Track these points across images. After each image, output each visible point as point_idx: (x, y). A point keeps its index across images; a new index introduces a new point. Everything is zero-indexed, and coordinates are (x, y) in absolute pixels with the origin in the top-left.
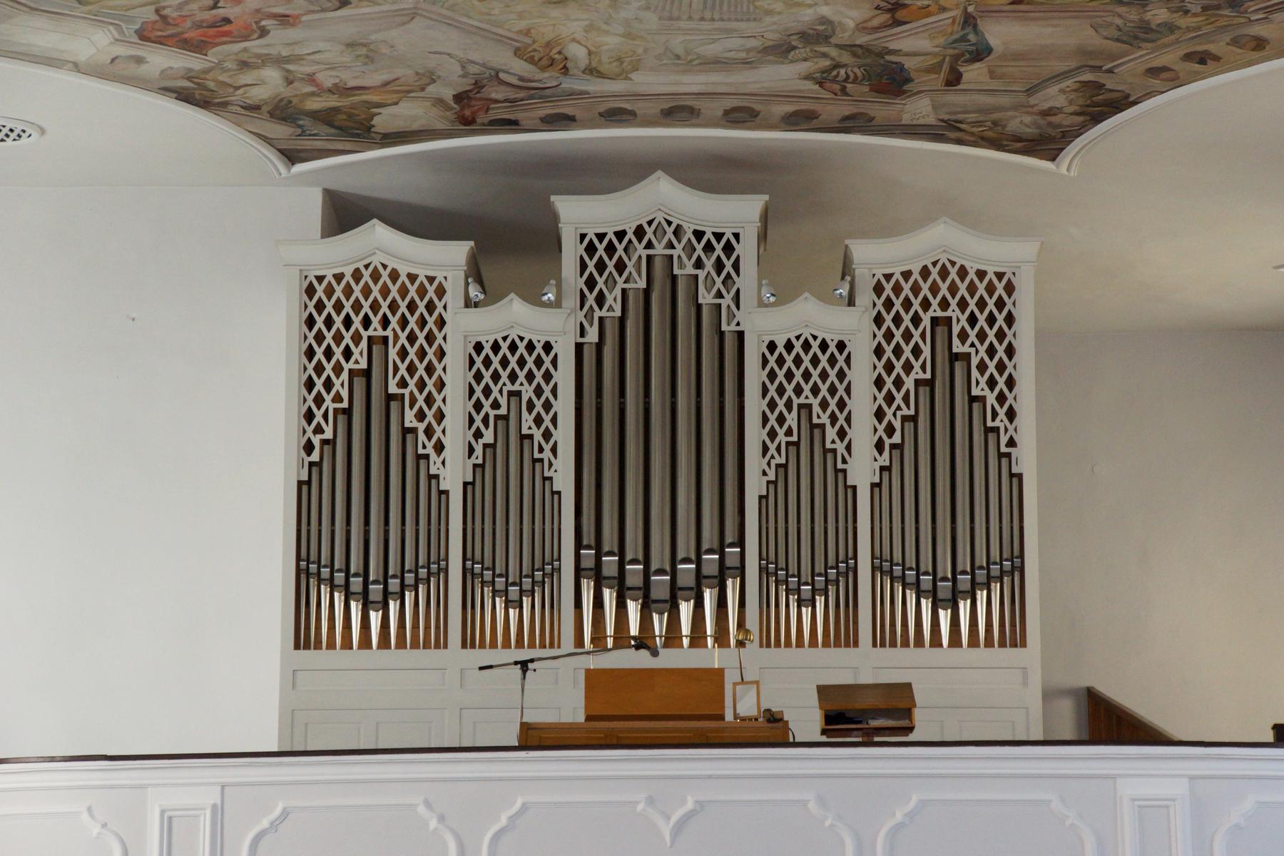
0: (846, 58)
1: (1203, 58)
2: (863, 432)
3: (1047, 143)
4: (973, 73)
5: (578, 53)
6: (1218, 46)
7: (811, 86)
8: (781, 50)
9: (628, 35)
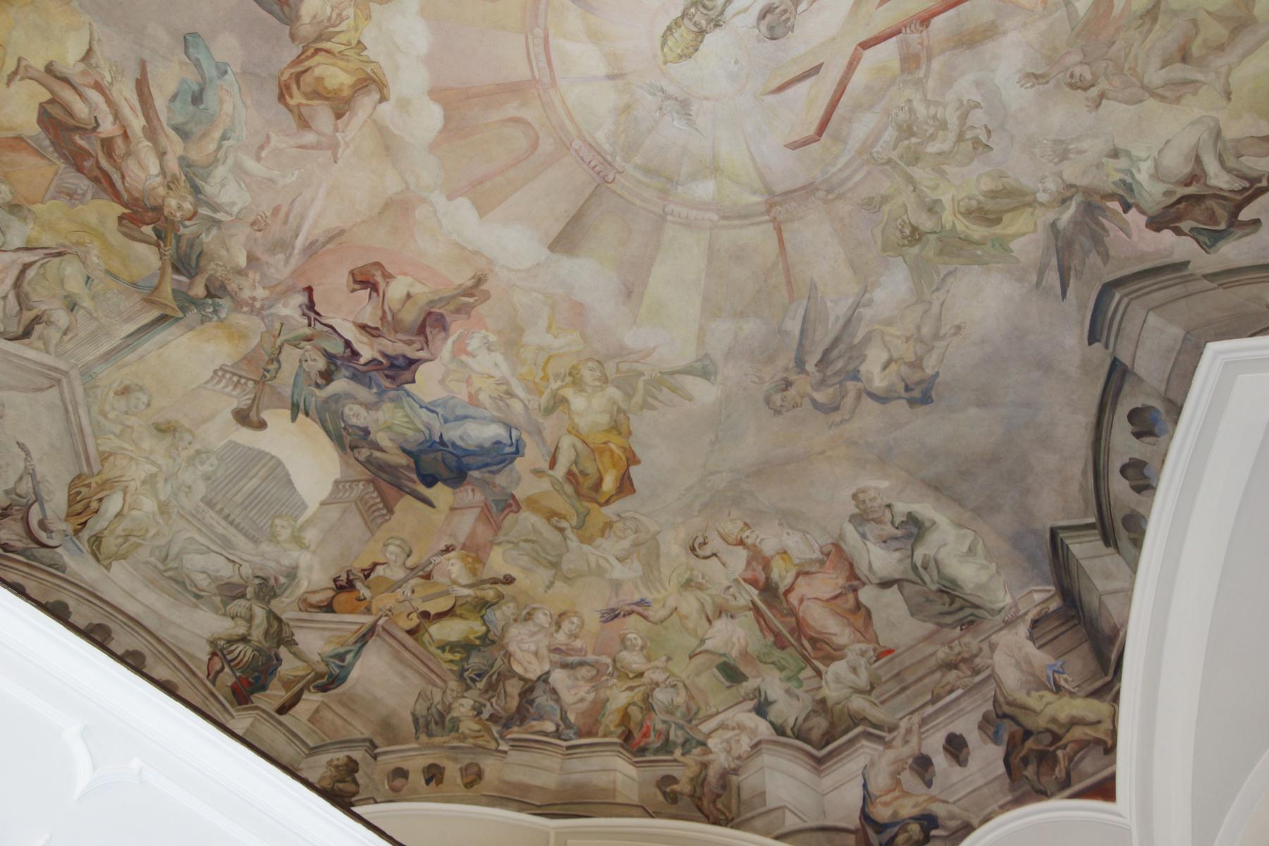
0: (257, 634)
1: (433, 775)
4: (312, 700)
5: (113, 504)
6: (452, 770)
7: (203, 653)
9: (164, 509)
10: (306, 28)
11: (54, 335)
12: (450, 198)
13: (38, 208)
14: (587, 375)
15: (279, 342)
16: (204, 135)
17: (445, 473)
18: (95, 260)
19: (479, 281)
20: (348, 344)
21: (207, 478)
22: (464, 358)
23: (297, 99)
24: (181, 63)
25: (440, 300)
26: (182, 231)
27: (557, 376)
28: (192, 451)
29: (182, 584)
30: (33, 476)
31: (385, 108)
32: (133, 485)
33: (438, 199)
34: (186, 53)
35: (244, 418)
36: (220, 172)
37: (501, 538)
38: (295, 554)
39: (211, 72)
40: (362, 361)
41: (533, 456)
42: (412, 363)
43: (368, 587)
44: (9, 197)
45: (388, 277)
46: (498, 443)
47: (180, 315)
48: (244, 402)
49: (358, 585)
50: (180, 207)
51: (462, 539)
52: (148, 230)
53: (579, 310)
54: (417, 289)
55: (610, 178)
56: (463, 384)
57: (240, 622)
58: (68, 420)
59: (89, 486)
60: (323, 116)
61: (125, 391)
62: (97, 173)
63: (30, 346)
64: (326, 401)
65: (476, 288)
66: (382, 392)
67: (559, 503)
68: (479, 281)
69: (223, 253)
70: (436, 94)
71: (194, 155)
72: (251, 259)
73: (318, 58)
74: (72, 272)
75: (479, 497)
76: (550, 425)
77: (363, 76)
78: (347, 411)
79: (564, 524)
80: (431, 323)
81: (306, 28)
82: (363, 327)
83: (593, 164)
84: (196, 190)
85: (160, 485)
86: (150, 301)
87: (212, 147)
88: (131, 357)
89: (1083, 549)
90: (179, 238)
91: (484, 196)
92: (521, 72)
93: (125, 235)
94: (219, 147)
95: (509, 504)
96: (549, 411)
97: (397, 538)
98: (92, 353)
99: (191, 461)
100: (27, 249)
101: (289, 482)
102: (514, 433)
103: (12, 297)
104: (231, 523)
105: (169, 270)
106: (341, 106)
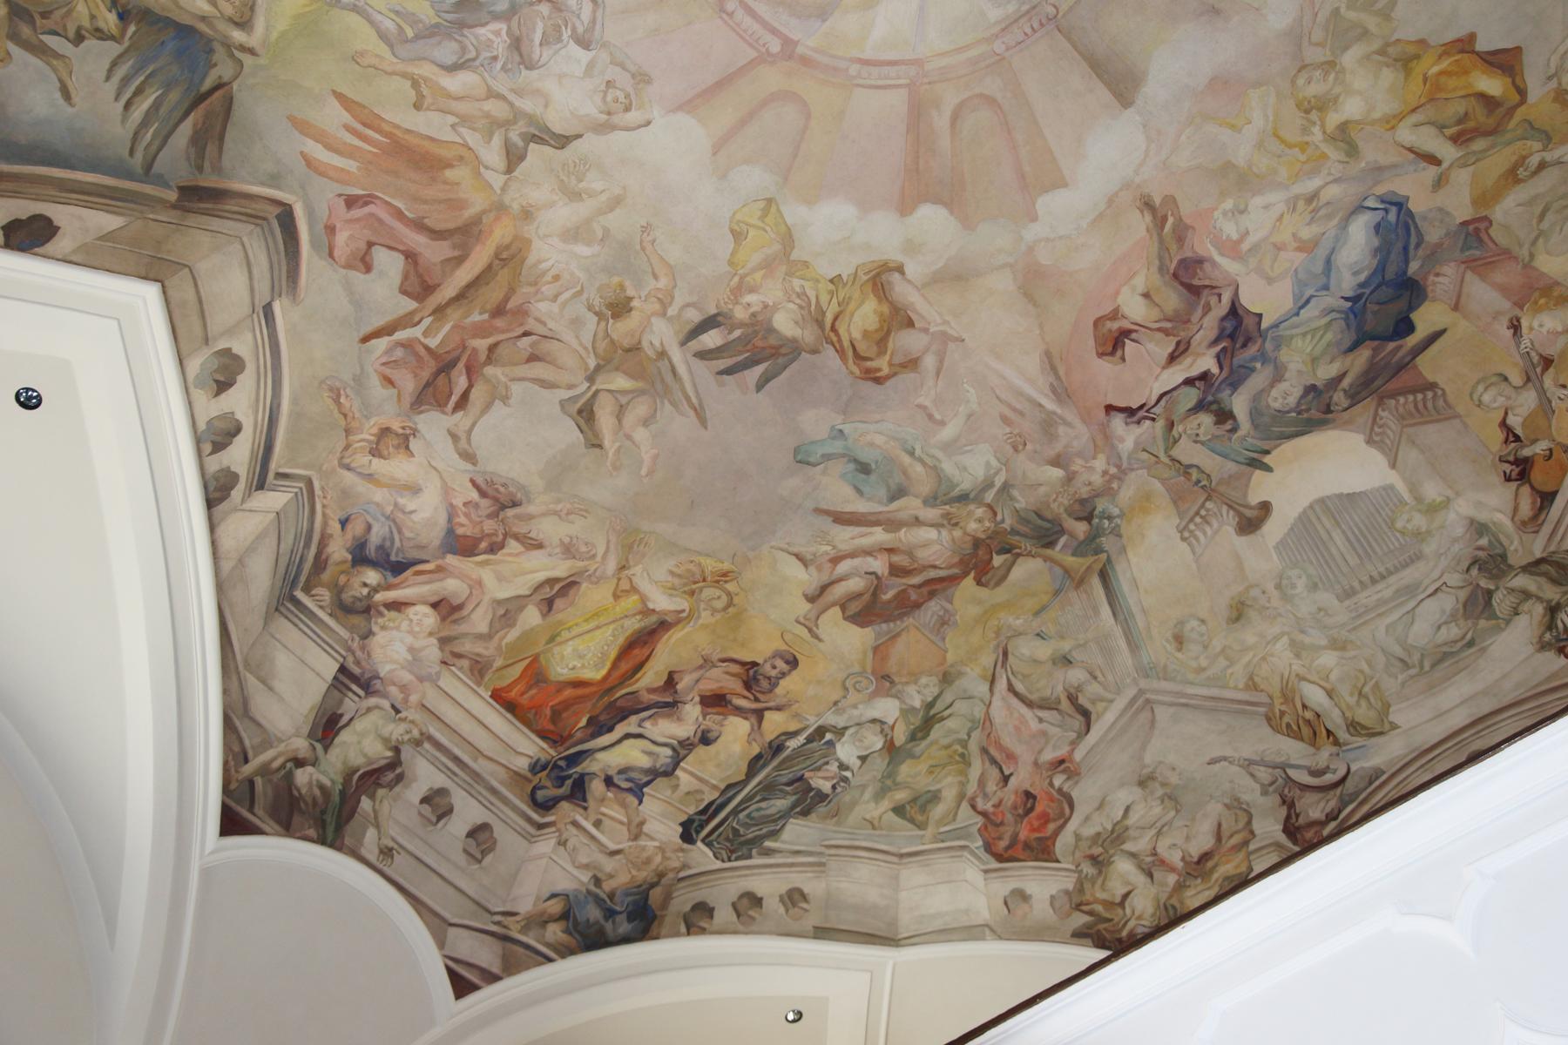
0: (1552, 593)
5: (1315, 696)
9: (1338, 645)
10: (807, 335)
11: (1094, 689)
12: (1034, 218)
13: (950, 657)
14: (1315, 88)
15: (1164, 458)
16: (905, 473)
17: (1402, 304)
18: (1018, 622)
19: (1147, 205)
20: (1189, 382)
21: (1314, 587)
22: (1245, 246)
23: (883, 364)
24: (824, 472)
25: (1161, 258)
26: (1007, 525)
27: (1305, 130)
28: (1275, 593)
29: (1445, 656)
30: (1251, 762)
31: (910, 270)
32: (1297, 667)
33: (1032, 232)
34: (814, 465)
35: (1252, 521)
36: (948, 467)
37: (1524, 253)
38: (1452, 516)
39: (837, 447)
40: (1215, 370)
41: (1414, 187)
42: (1235, 311)
43: (1534, 441)
44: (934, 680)
45: (1115, 314)
46: (1377, 228)
47: (1104, 556)
48: (1231, 519)
49: (1526, 452)
50: (980, 521)
51: (1506, 305)
52: (998, 560)
53: (1224, 85)
54: (1140, 282)
55: (1051, 10)
56: (1283, 252)
57: (1526, 606)
58: (1195, 707)
59: (1282, 713)
60: (906, 342)
61: (1179, 640)
62: (925, 590)
63: (1099, 717)
64: (1255, 426)
65: (1157, 211)
66: (1263, 357)
67: (1498, 160)
68: (1147, 205)
69: (1042, 490)
70: (905, 207)
71: (926, 489)
72: (1056, 462)
73: (842, 331)
74: (1026, 648)
75: (1450, 270)
76: (1371, 153)
77: (870, 286)
78: (1277, 405)
79: (1534, 161)
80: (1189, 277)
81: (807, 335)
82: (1172, 359)
83: (1029, 31)
84: (963, 498)
85: (1307, 640)
86: (1080, 583)
87: (919, 468)
88: (1140, 621)
90: (1014, 532)
91: (1043, 176)
92: (897, 101)
93: (998, 584)
94: (921, 460)
95: (1474, 232)
96: (1352, 151)
97: (1474, 387)
98: (1124, 657)
99: (1286, 598)
100: (992, 682)
101: (1351, 497)
102: (1371, 203)
103: (1041, 713)
104: (1383, 577)
105: (1048, 552)
106: (899, 318)
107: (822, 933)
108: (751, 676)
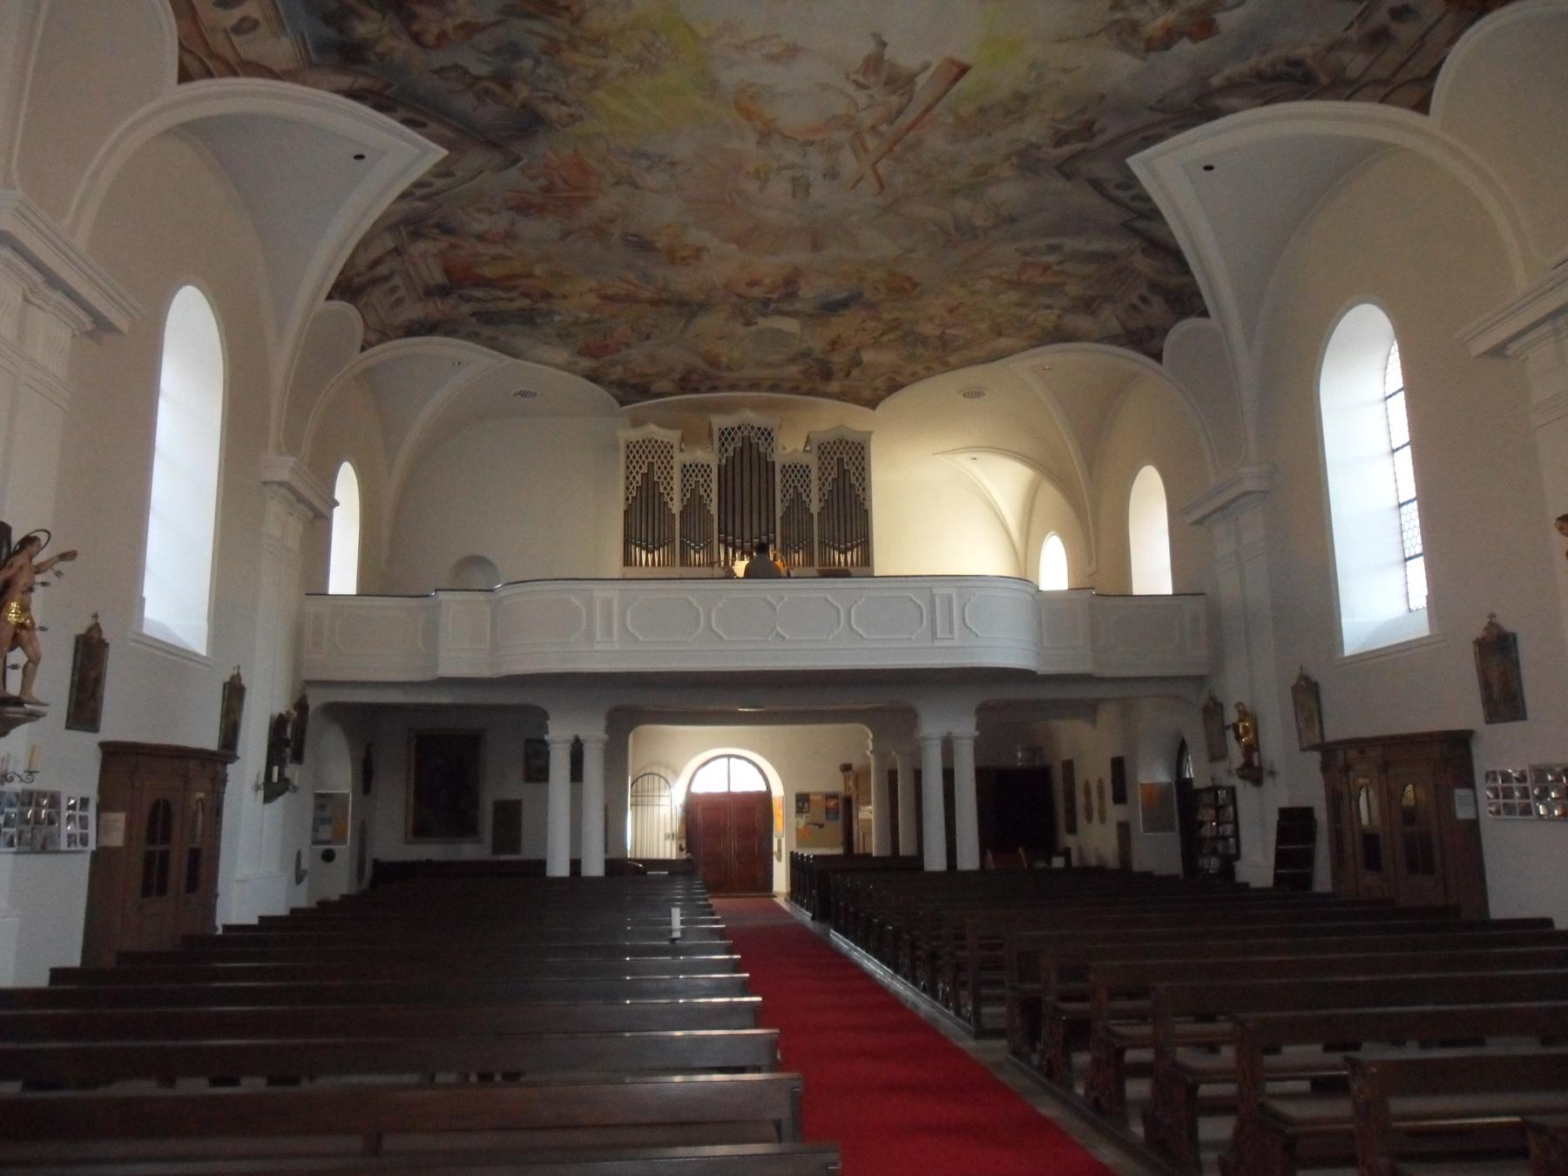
2: (815, 495)
3: (872, 404)
4: (855, 372)
5: (724, 360)
8: (792, 360)
35: (748, 324)
89: (1140, 224)
107: (492, 347)
108: (547, 296)
